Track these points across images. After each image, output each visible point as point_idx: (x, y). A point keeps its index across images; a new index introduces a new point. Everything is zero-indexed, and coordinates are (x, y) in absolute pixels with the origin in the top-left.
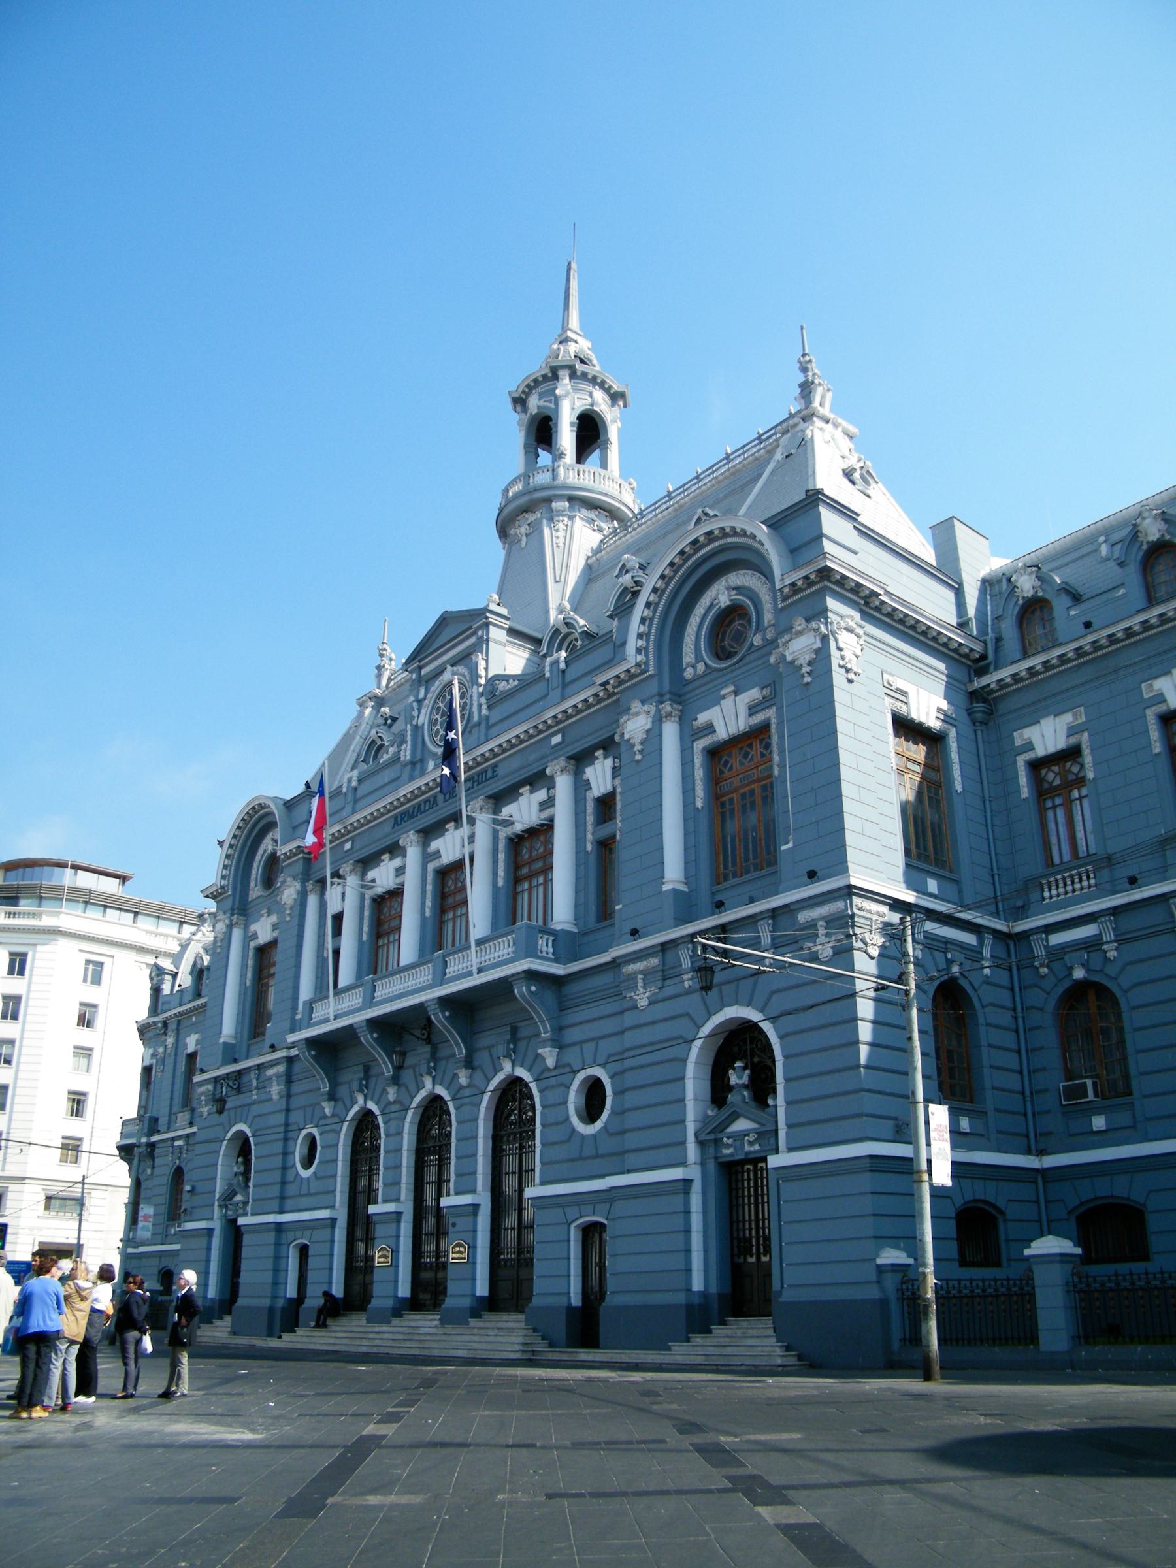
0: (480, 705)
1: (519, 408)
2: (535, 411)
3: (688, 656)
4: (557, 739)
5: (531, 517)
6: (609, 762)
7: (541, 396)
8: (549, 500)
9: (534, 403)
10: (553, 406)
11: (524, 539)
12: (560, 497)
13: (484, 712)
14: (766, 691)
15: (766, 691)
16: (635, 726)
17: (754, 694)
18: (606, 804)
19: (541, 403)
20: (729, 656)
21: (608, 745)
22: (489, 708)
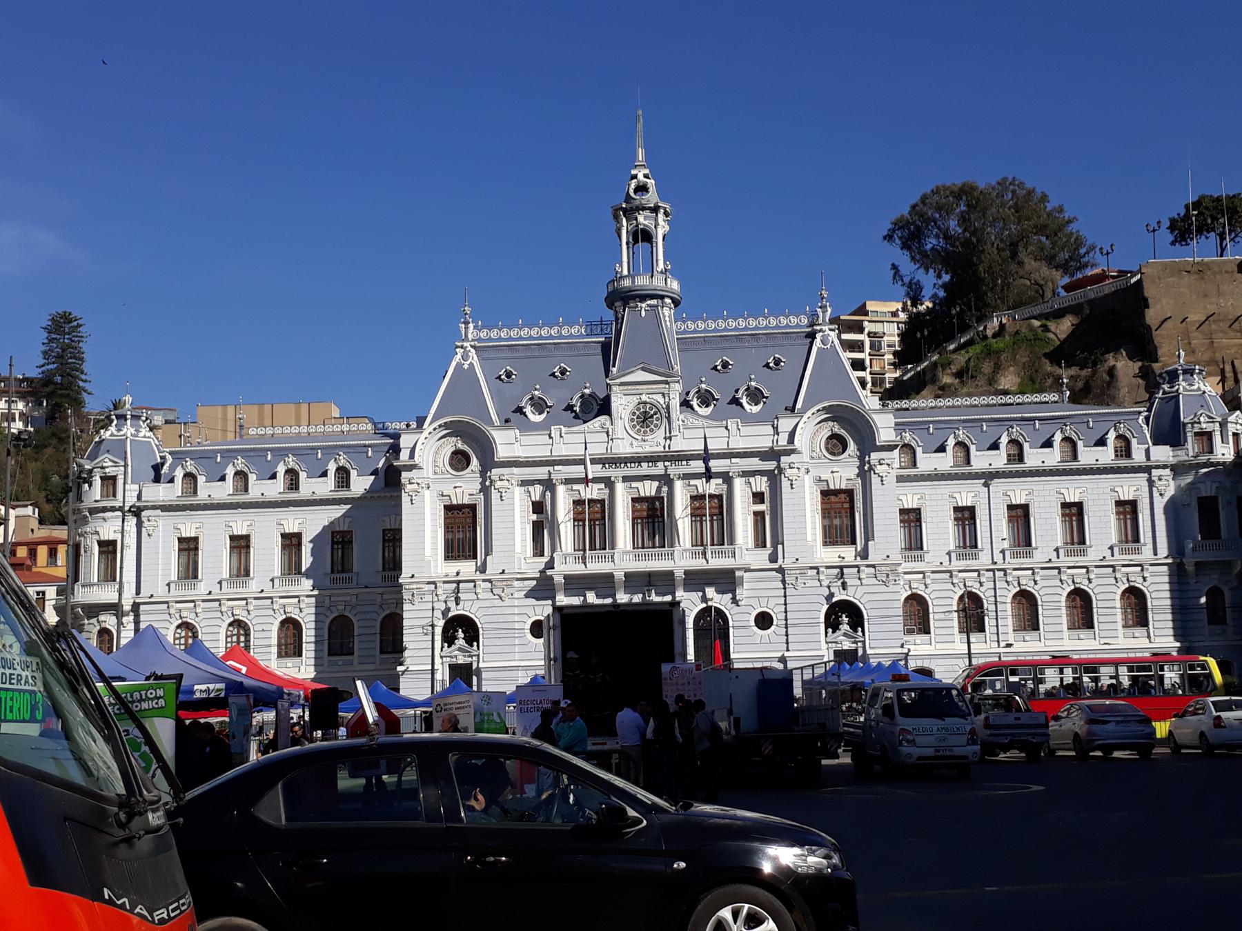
8: (662, 297)
11: (643, 313)
19: (646, 222)
20: (832, 454)
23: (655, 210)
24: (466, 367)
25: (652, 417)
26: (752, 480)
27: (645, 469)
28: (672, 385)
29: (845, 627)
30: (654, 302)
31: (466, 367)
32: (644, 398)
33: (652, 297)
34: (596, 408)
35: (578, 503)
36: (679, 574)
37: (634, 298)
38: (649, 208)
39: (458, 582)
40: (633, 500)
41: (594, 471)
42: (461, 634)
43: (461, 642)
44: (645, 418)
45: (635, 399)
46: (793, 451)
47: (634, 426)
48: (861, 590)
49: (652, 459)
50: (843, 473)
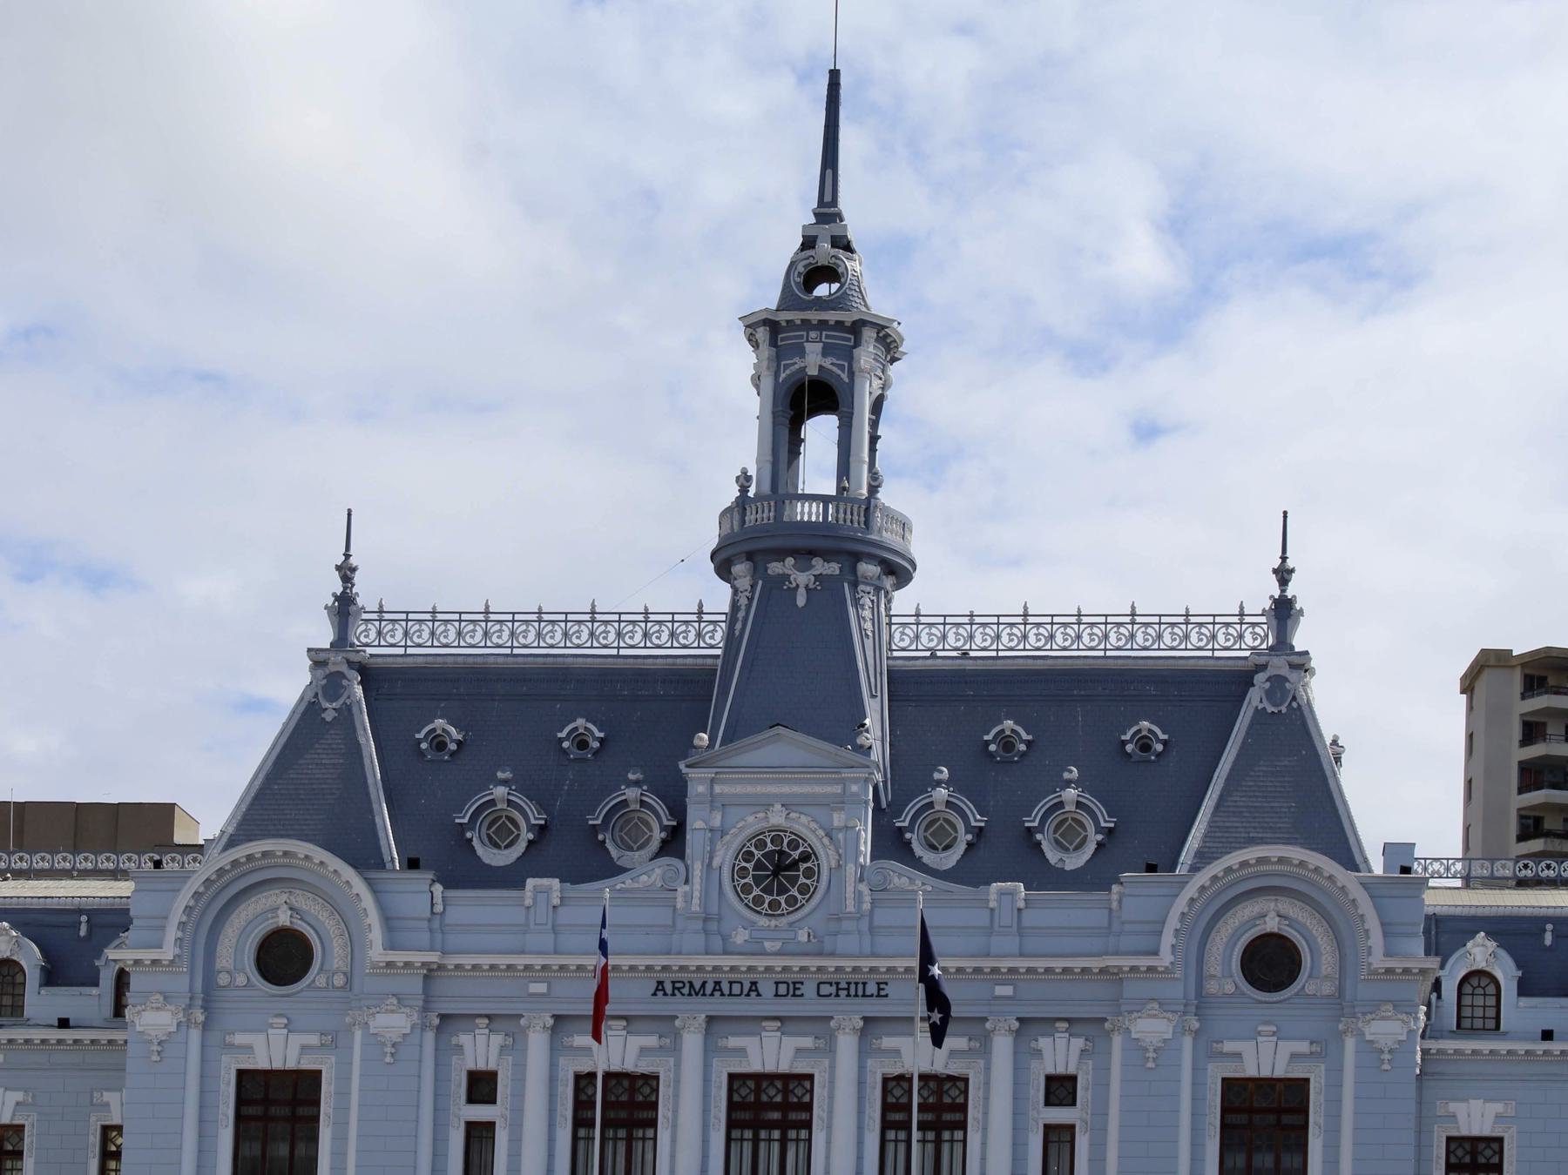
0: (859, 896)
1: (762, 334)
2: (813, 371)
3: (1214, 966)
4: (1001, 991)
5: (820, 566)
6: (1077, 1043)
7: (825, 354)
8: (857, 557)
9: (813, 360)
10: (845, 377)
12: (871, 558)
13: (867, 906)
14: (1315, 1048)
15: (1315, 1048)
16: (1152, 1028)
17: (1303, 1047)
18: (1060, 1089)
19: (827, 363)
21: (1091, 1027)
22: (873, 902)
23: (856, 328)
24: (329, 716)
25: (794, 865)
30: (833, 568)
31: (329, 716)
32: (777, 818)
33: (827, 555)
34: (658, 835)
35: (583, 1081)
37: (780, 554)
38: (839, 325)
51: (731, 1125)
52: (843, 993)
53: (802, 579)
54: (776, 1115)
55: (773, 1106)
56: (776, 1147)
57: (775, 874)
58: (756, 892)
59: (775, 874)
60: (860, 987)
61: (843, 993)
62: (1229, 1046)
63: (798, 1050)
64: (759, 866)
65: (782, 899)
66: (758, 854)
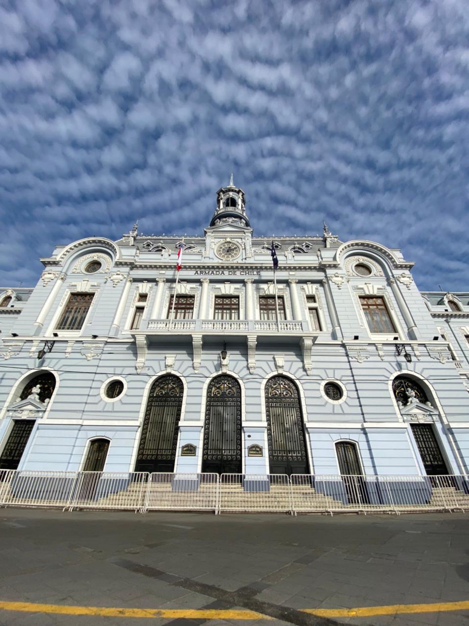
1: (221, 193)
12: (244, 219)
18: (311, 298)
19: (233, 195)
25: (233, 250)
26: (305, 286)
27: (227, 275)
28: (247, 234)
29: (414, 401)
32: (228, 240)
36: (252, 341)
39: (54, 342)
40: (217, 297)
41: (190, 274)
42: (36, 389)
43: (34, 397)
44: (229, 250)
45: (222, 241)
46: (335, 266)
47: (221, 254)
48: (419, 367)
49: (232, 269)
50: (374, 285)
51: (215, 309)
52: (247, 274)
53: (230, 220)
54: (227, 307)
55: (227, 304)
56: (228, 315)
57: (228, 251)
58: (223, 254)
59: (228, 251)
60: (252, 273)
61: (247, 274)
62: (360, 286)
63: (235, 288)
64: (223, 250)
65: (230, 256)
66: (223, 248)
